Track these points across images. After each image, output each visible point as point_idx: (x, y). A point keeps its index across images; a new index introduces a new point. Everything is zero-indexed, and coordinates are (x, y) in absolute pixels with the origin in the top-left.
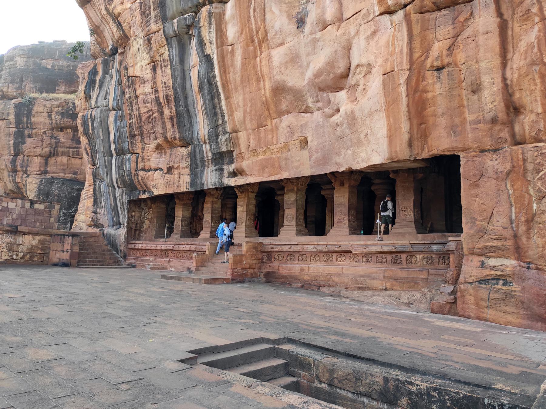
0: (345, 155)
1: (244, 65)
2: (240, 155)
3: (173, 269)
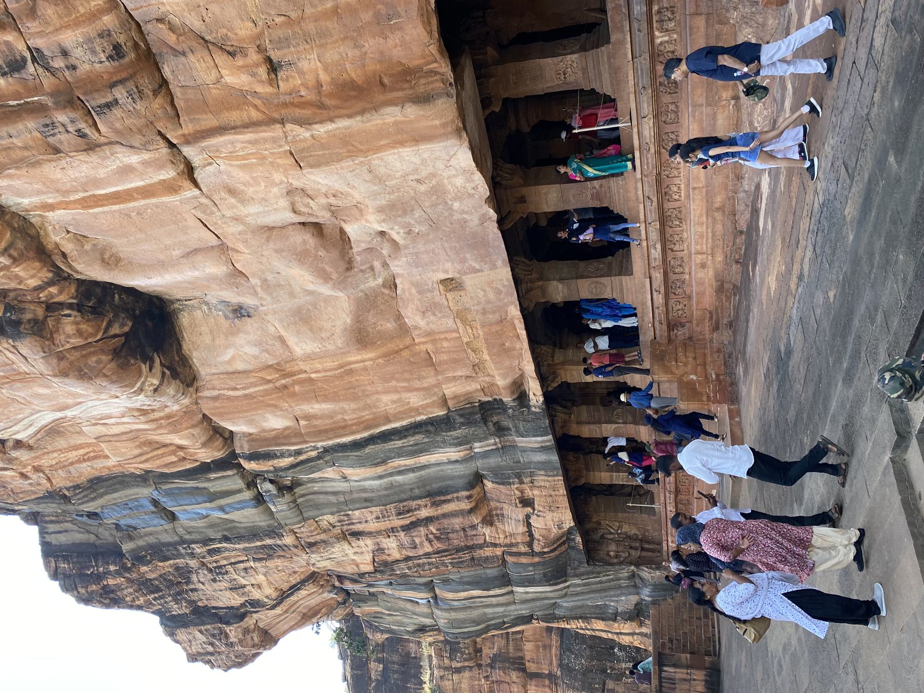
0: (463, 212)
1: (326, 399)
2: (486, 390)
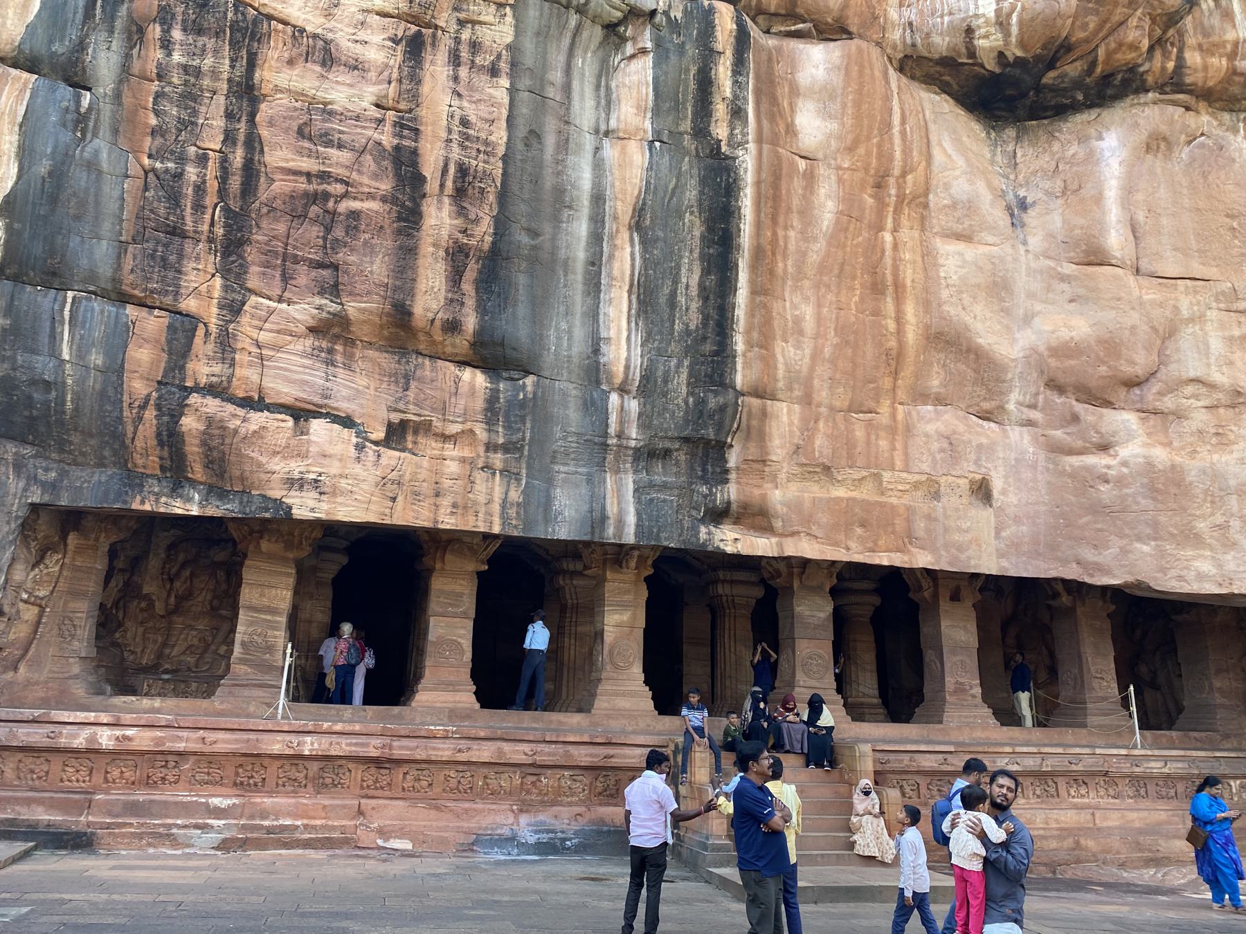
1: (840, 228)
2: (756, 466)
3: (405, 845)
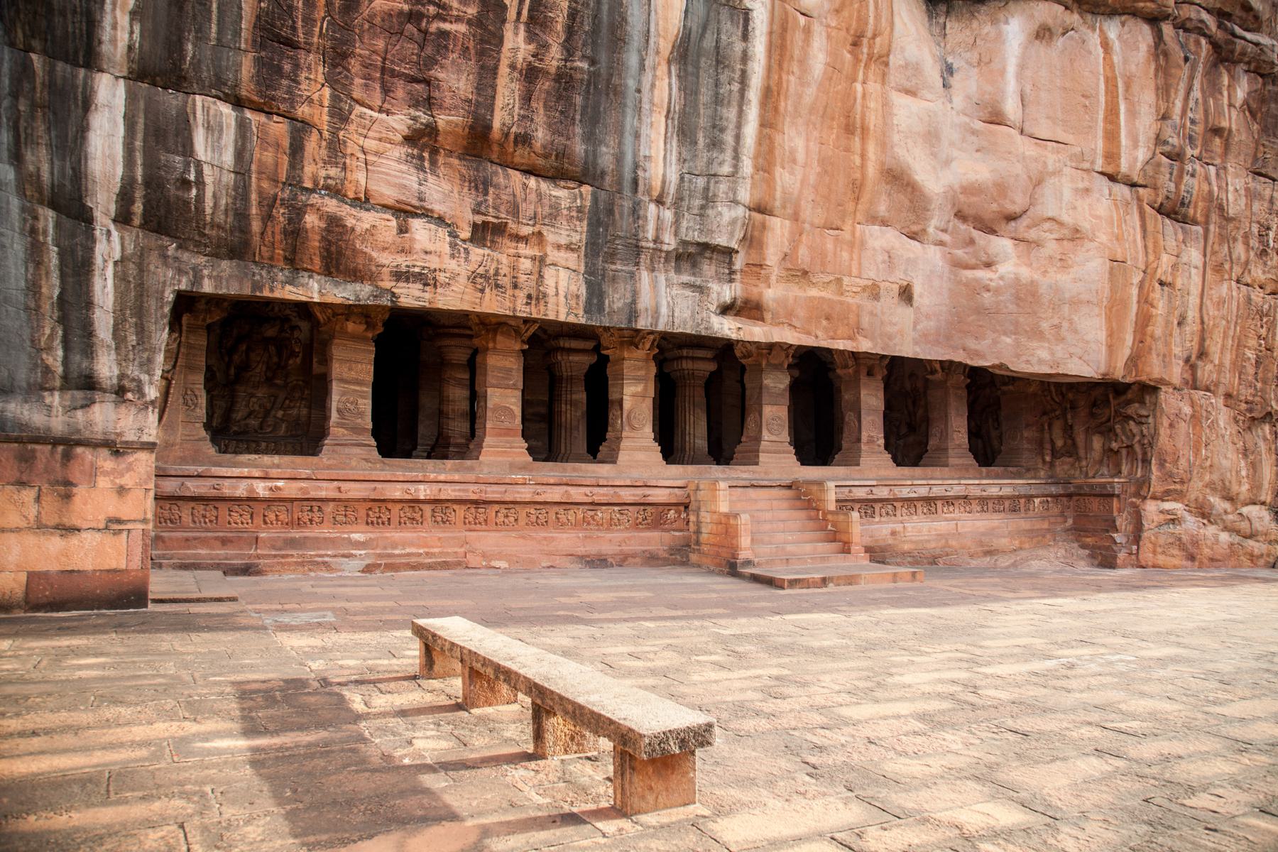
2: (754, 269)
